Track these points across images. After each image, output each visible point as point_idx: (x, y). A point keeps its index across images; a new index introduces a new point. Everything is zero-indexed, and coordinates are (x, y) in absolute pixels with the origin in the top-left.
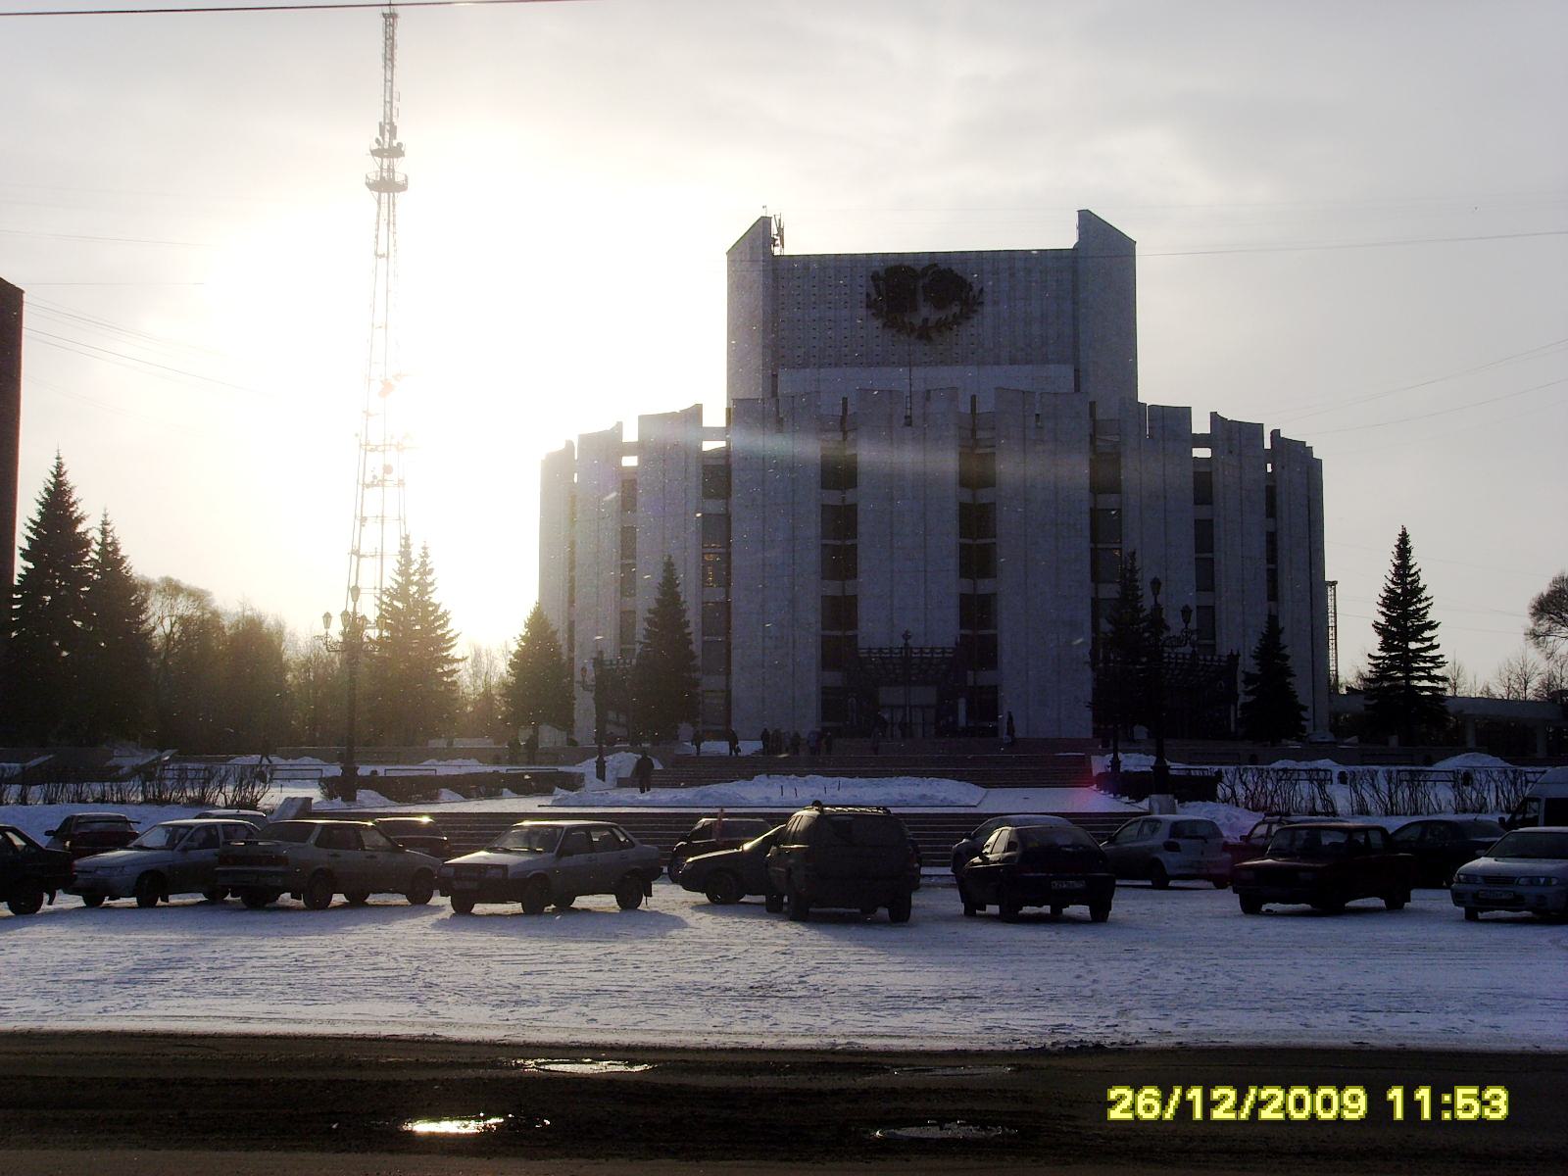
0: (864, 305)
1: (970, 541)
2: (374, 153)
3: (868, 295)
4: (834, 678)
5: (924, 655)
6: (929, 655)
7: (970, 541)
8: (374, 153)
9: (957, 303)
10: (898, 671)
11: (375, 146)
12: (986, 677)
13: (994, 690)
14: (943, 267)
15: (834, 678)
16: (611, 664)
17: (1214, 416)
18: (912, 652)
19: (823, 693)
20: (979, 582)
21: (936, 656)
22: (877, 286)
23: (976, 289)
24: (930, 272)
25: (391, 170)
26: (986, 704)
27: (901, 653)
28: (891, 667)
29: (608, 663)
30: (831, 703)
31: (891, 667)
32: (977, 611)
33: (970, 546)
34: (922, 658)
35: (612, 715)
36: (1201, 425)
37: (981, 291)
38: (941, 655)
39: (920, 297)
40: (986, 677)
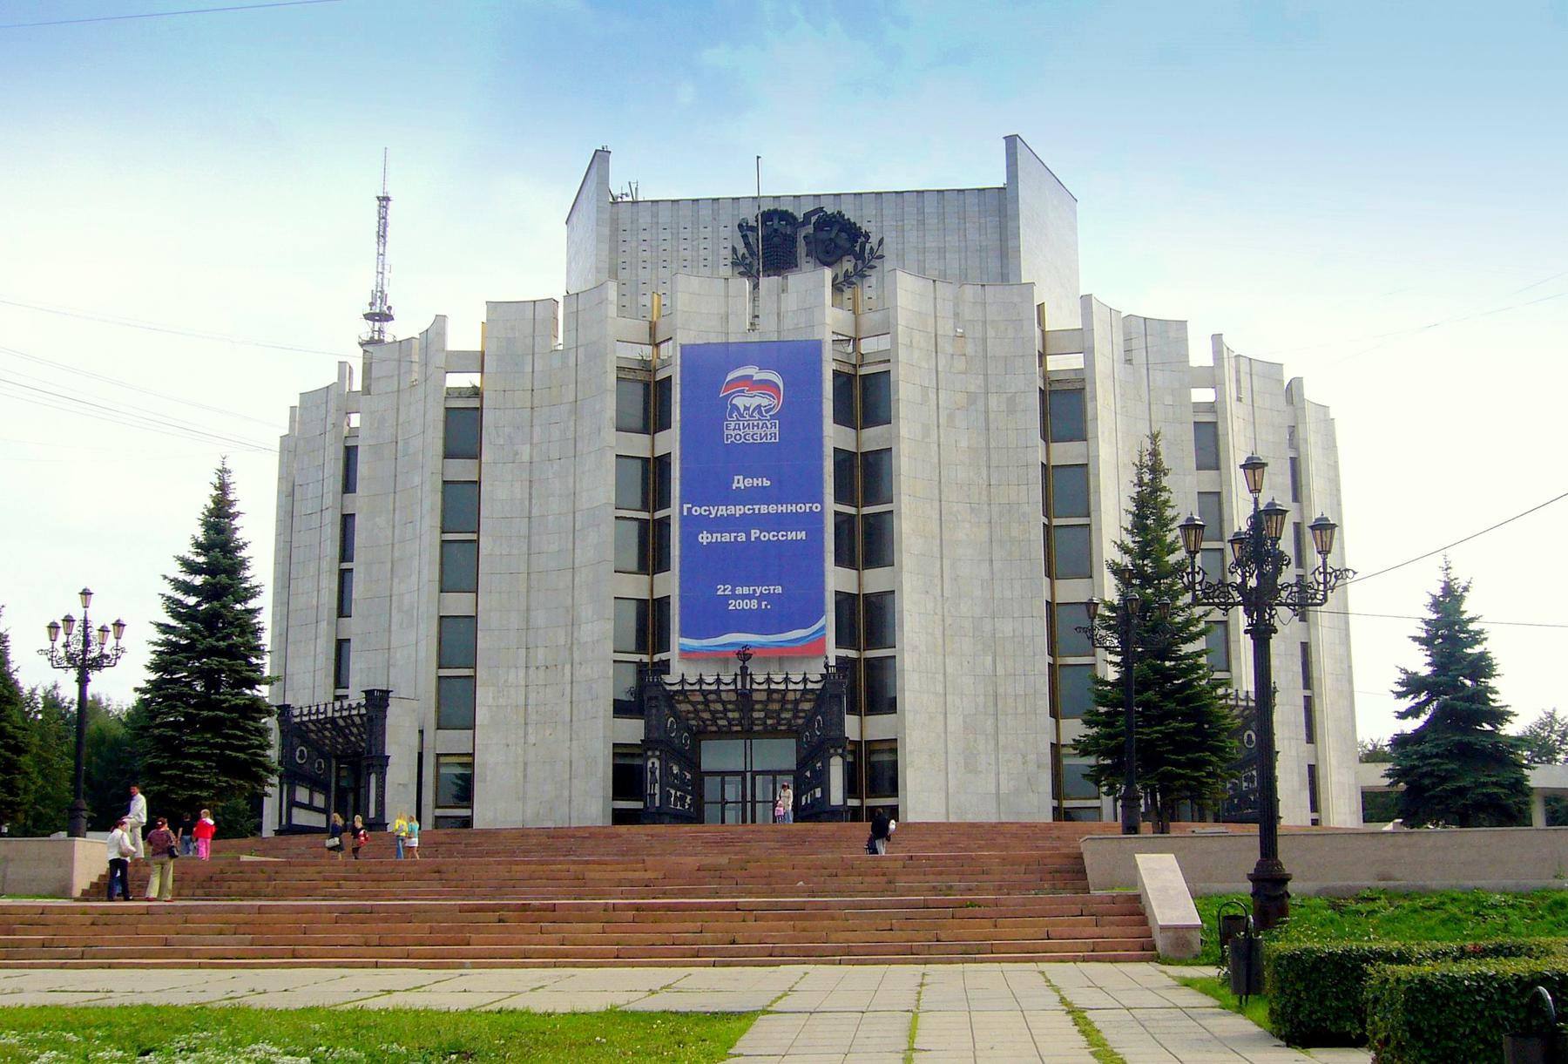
0: (729, 262)
1: (852, 510)
2: (368, 317)
3: (734, 249)
4: (632, 730)
5: (773, 686)
6: (782, 687)
7: (852, 510)
8: (368, 317)
9: (851, 257)
10: (730, 715)
11: (368, 311)
12: (877, 727)
13: (891, 746)
14: (830, 210)
15: (632, 730)
16: (302, 714)
17: (1217, 339)
18: (752, 681)
19: (615, 754)
20: (869, 574)
21: (791, 687)
22: (744, 237)
23: (874, 240)
24: (813, 219)
25: (380, 331)
26: (877, 772)
27: (735, 681)
28: (719, 707)
29: (297, 712)
30: (627, 776)
31: (719, 707)
32: (868, 620)
33: (851, 518)
34: (770, 692)
35: (302, 794)
36: (1200, 355)
37: (881, 242)
38: (801, 687)
39: (801, 248)
40: (877, 727)
